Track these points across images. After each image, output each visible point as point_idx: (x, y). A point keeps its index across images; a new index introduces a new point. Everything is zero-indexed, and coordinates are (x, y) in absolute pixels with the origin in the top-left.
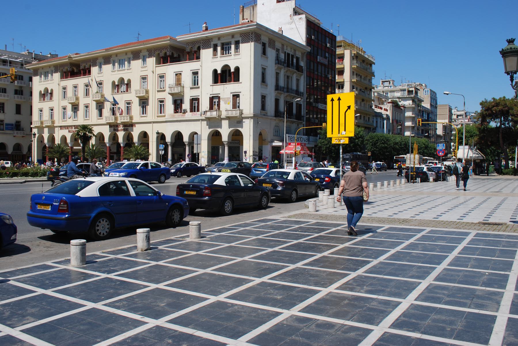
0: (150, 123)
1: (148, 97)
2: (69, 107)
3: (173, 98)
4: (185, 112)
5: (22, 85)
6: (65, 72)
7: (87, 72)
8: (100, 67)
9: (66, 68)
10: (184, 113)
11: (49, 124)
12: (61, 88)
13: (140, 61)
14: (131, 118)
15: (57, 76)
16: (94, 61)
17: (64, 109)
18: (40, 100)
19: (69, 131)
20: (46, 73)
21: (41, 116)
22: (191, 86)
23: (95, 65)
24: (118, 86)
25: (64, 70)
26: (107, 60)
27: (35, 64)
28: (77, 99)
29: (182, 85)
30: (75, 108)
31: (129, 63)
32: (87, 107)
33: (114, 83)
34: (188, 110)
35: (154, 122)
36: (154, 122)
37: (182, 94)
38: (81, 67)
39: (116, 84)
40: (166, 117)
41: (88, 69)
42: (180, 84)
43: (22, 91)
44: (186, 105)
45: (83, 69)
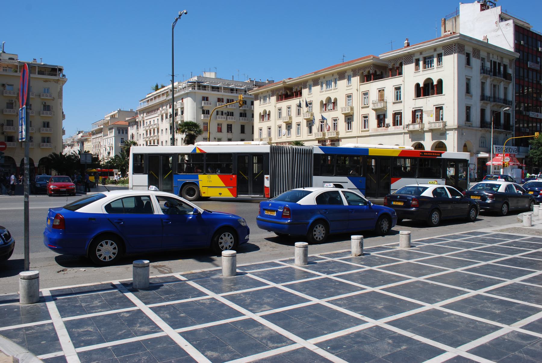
2: (284, 126)
4: (388, 126)
5: (246, 109)
6: (280, 96)
7: (299, 94)
8: (310, 89)
9: (281, 91)
10: (387, 127)
13: (345, 81)
14: (338, 133)
15: (274, 99)
16: (304, 84)
17: (280, 127)
18: (260, 120)
20: (264, 97)
22: (394, 101)
24: (325, 104)
25: (280, 94)
26: (316, 82)
28: (290, 118)
29: (385, 101)
30: (289, 126)
31: (336, 83)
32: (299, 125)
33: (322, 102)
34: (391, 124)
35: (358, 137)
36: (358, 137)
37: (385, 109)
38: (294, 90)
39: (324, 103)
40: (370, 131)
42: (383, 100)
43: (246, 114)
44: (389, 120)
45: (295, 92)
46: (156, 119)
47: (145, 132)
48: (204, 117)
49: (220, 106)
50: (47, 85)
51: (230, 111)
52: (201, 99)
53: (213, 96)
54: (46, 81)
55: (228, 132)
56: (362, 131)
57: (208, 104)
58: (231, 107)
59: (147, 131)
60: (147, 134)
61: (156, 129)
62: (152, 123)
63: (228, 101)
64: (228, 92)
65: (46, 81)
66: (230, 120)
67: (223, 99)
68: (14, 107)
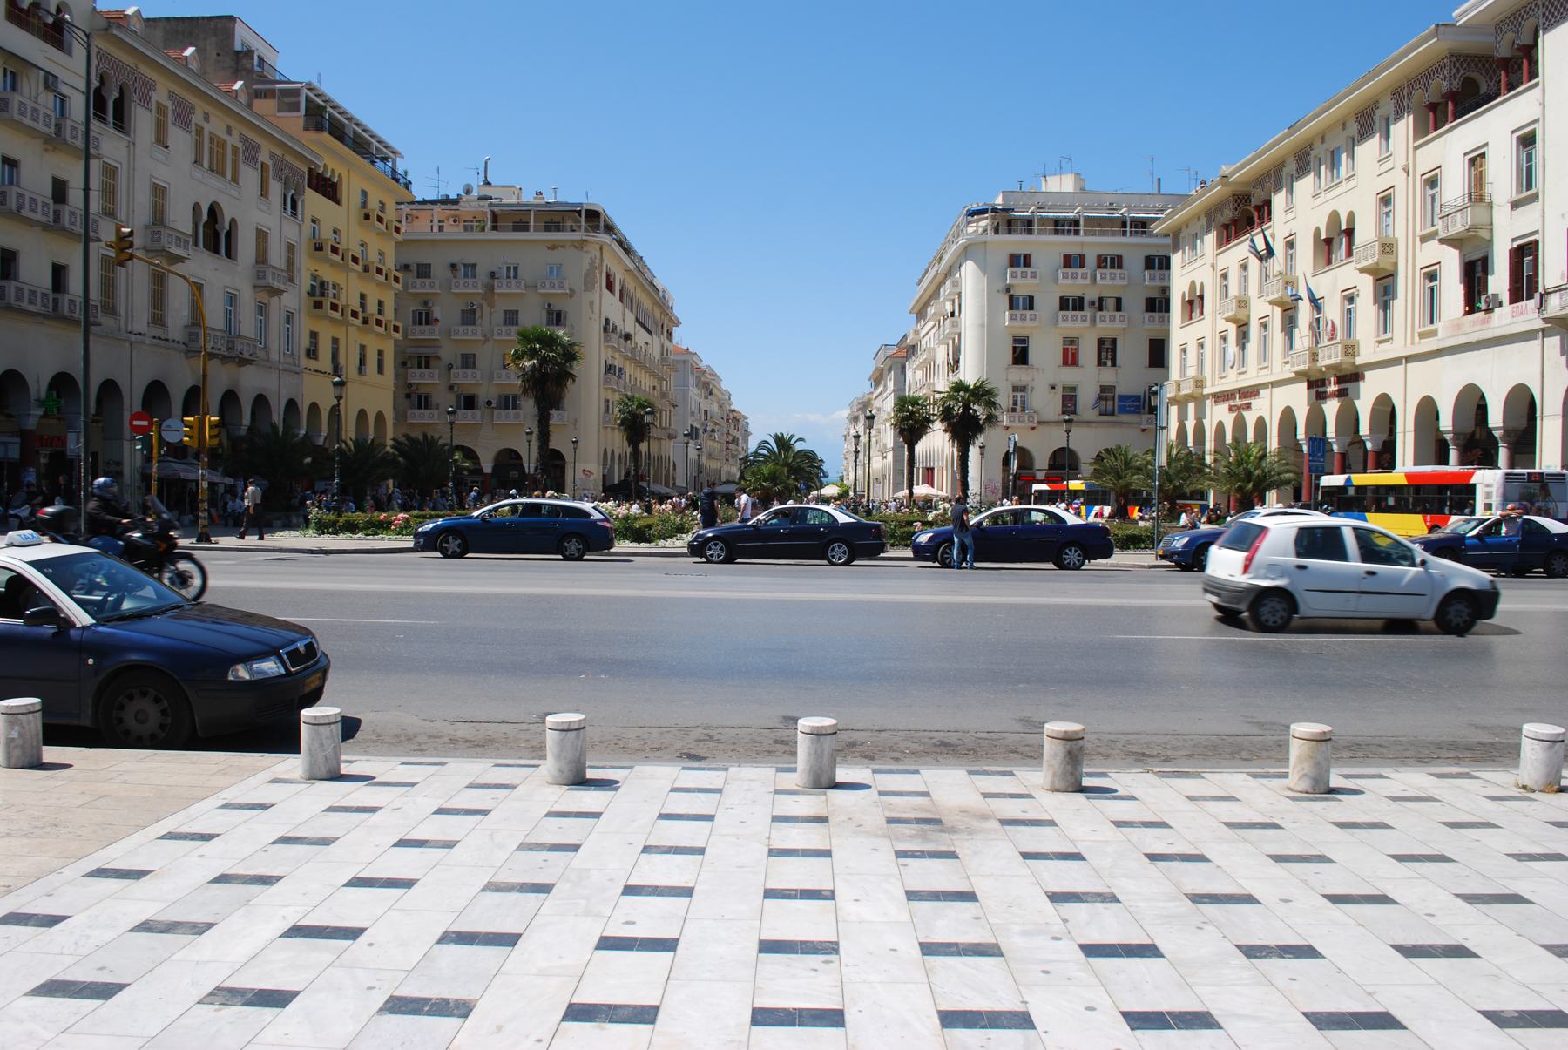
0: (1395, 362)
1: (1396, 264)
3: (1462, 256)
10: (1489, 311)
13: (1374, 142)
14: (1350, 349)
16: (1276, 176)
19: (1231, 409)
22: (1515, 197)
23: (1277, 189)
26: (1303, 160)
27: (1168, 217)
29: (1487, 199)
31: (1352, 156)
35: (1409, 359)
36: (1409, 359)
37: (1484, 234)
38: (1254, 201)
42: (1480, 198)
44: (1499, 281)
48: (1013, 318)
49: (1076, 284)
50: (556, 257)
52: (1005, 260)
53: (1047, 248)
54: (553, 246)
55: (1100, 363)
56: (1422, 336)
57: (1024, 275)
58: (1108, 282)
63: (1102, 262)
64: (1114, 234)
65: (553, 246)
66: (1108, 325)
67: (1082, 257)
68: (478, 321)
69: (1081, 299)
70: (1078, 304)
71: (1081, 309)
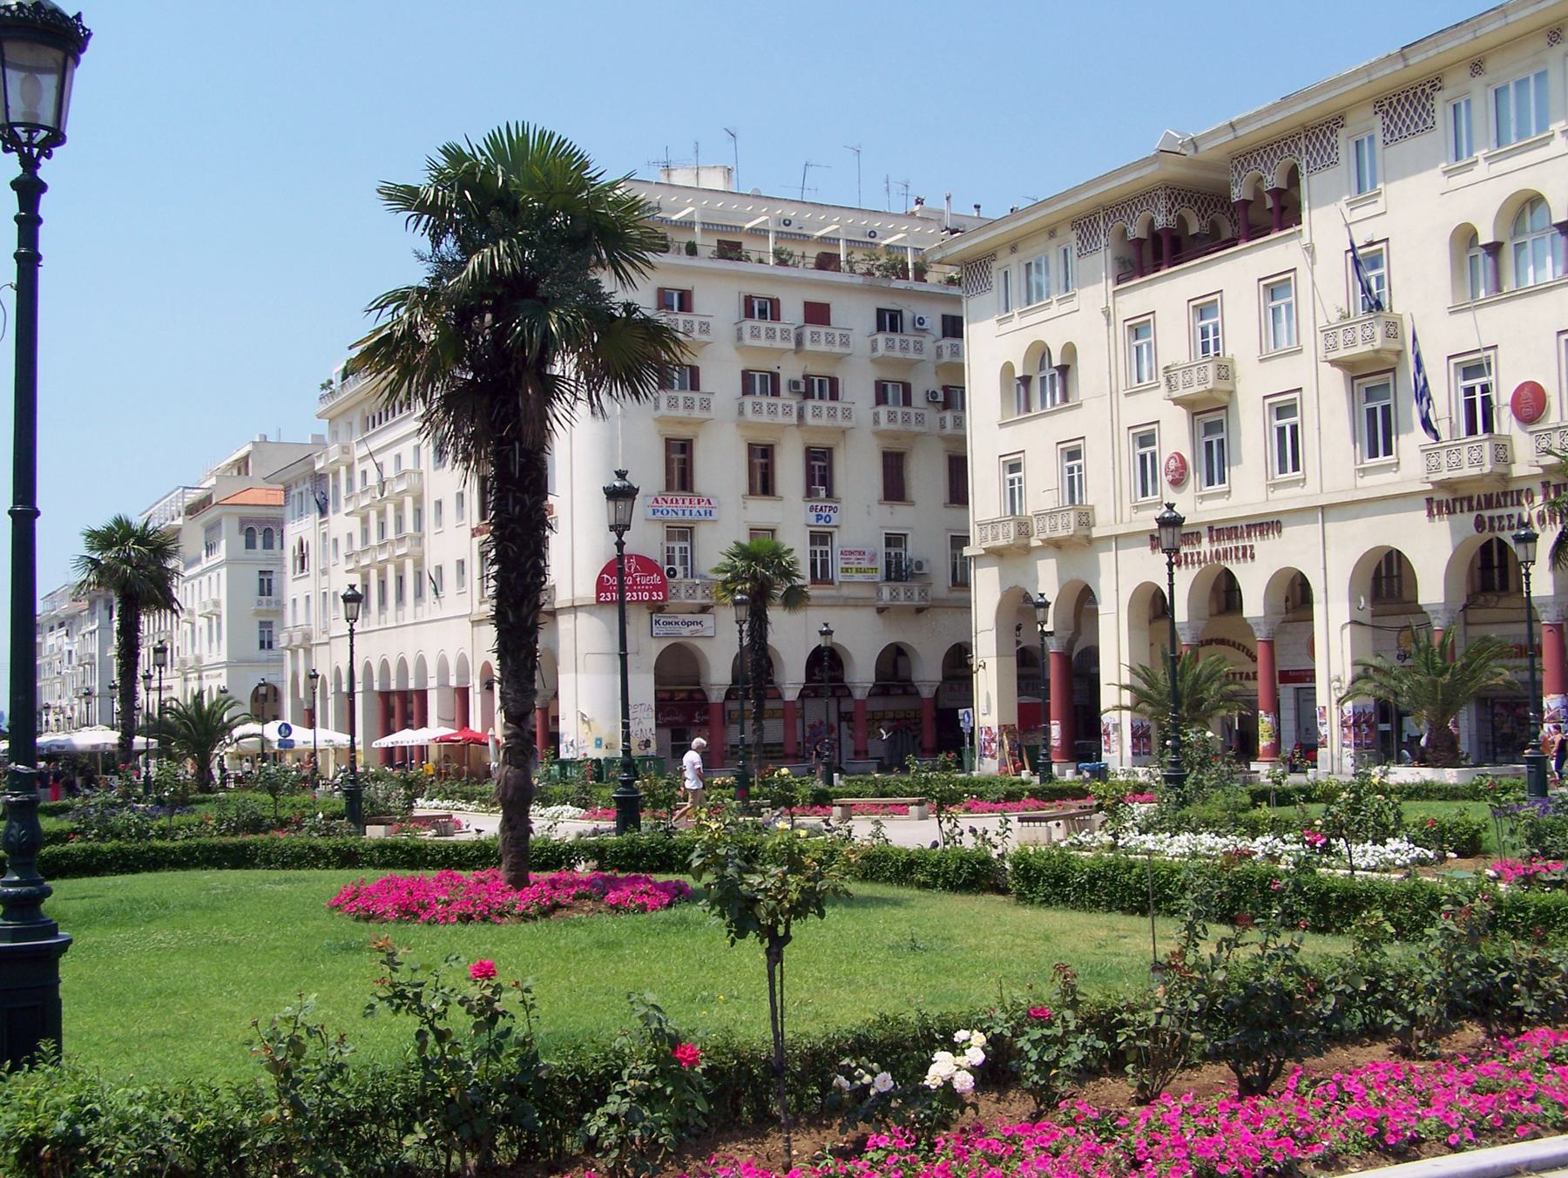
7: (1281, 211)
11: (1065, 528)
12: (1121, 330)
17: (1146, 439)
21: (1014, 495)
24: (1494, 249)
25: (1137, 231)
28: (1225, 371)
33: (1465, 237)
41: (1277, 193)
46: (406, 449)
47: (355, 522)
51: (815, 369)
55: (810, 493)
59: (365, 520)
60: (365, 533)
61: (409, 503)
62: (390, 472)
69: (775, 377)
70: (772, 384)
71: (776, 392)
